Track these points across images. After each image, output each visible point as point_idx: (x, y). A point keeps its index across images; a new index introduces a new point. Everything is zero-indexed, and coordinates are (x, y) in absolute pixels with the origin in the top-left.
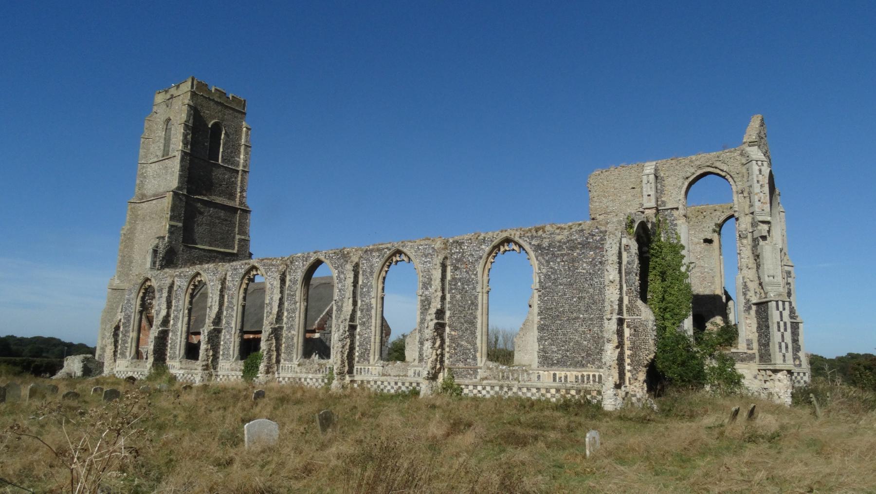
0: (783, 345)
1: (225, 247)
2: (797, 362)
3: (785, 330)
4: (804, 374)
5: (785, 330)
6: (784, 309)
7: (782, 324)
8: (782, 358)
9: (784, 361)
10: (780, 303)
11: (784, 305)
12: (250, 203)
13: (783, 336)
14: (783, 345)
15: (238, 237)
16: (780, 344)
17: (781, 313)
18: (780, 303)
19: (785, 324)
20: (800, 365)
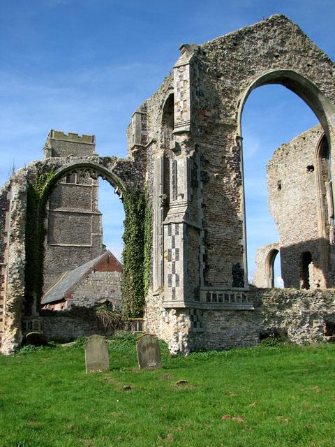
0: (174, 277)
1: (83, 243)
3: (177, 258)
5: (177, 258)
6: (177, 233)
7: (174, 251)
8: (171, 294)
10: (173, 226)
11: (177, 228)
12: (100, 208)
13: (174, 265)
14: (174, 277)
15: (92, 234)
16: (170, 276)
18: (173, 226)
19: (177, 251)
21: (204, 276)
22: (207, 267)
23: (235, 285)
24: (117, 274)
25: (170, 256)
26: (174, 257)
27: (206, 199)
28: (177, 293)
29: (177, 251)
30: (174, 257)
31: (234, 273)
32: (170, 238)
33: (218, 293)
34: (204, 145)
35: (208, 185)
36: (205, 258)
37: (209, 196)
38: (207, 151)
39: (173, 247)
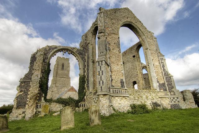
0: (101, 82)
2: (172, 93)
4: (178, 98)
5: (102, 74)
8: (100, 89)
9: (102, 90)
10: (100, 62)
13: (101, 77)
14: (101, 82)
17: (100, 67)
18: (100, 62)
19: (102, 72)
20: (175, 94)
21: (111, 83)
22: (112, 80)
24: (74, 93)
25: (99, 73)
26: (101, 74)
28: (103, 88)
29: (102, 72)
30: (101, 74)
31: (121, 82)
32: (99, 67)
33: (116, 90)
36: (111, 76)
39: (101, 70)
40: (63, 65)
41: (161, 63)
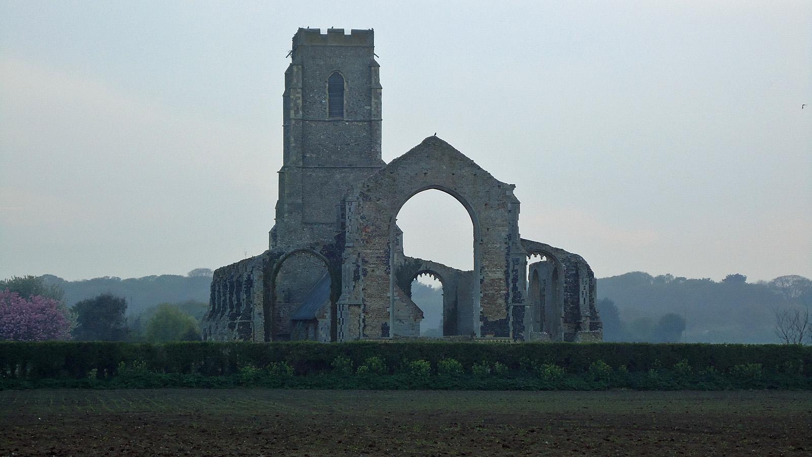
10: (341, 306)
18: (341, 306)
21: (363, 331)
22: (365, 326)
23: (383, 335)
27: (365, 285)
34: (365, 251)
35: (367, 277)
36: (364, 320)
37: (367, 283)
38: (367, 254)
39: (341, 317)
40: (336, 89)
41: (513, 271)
